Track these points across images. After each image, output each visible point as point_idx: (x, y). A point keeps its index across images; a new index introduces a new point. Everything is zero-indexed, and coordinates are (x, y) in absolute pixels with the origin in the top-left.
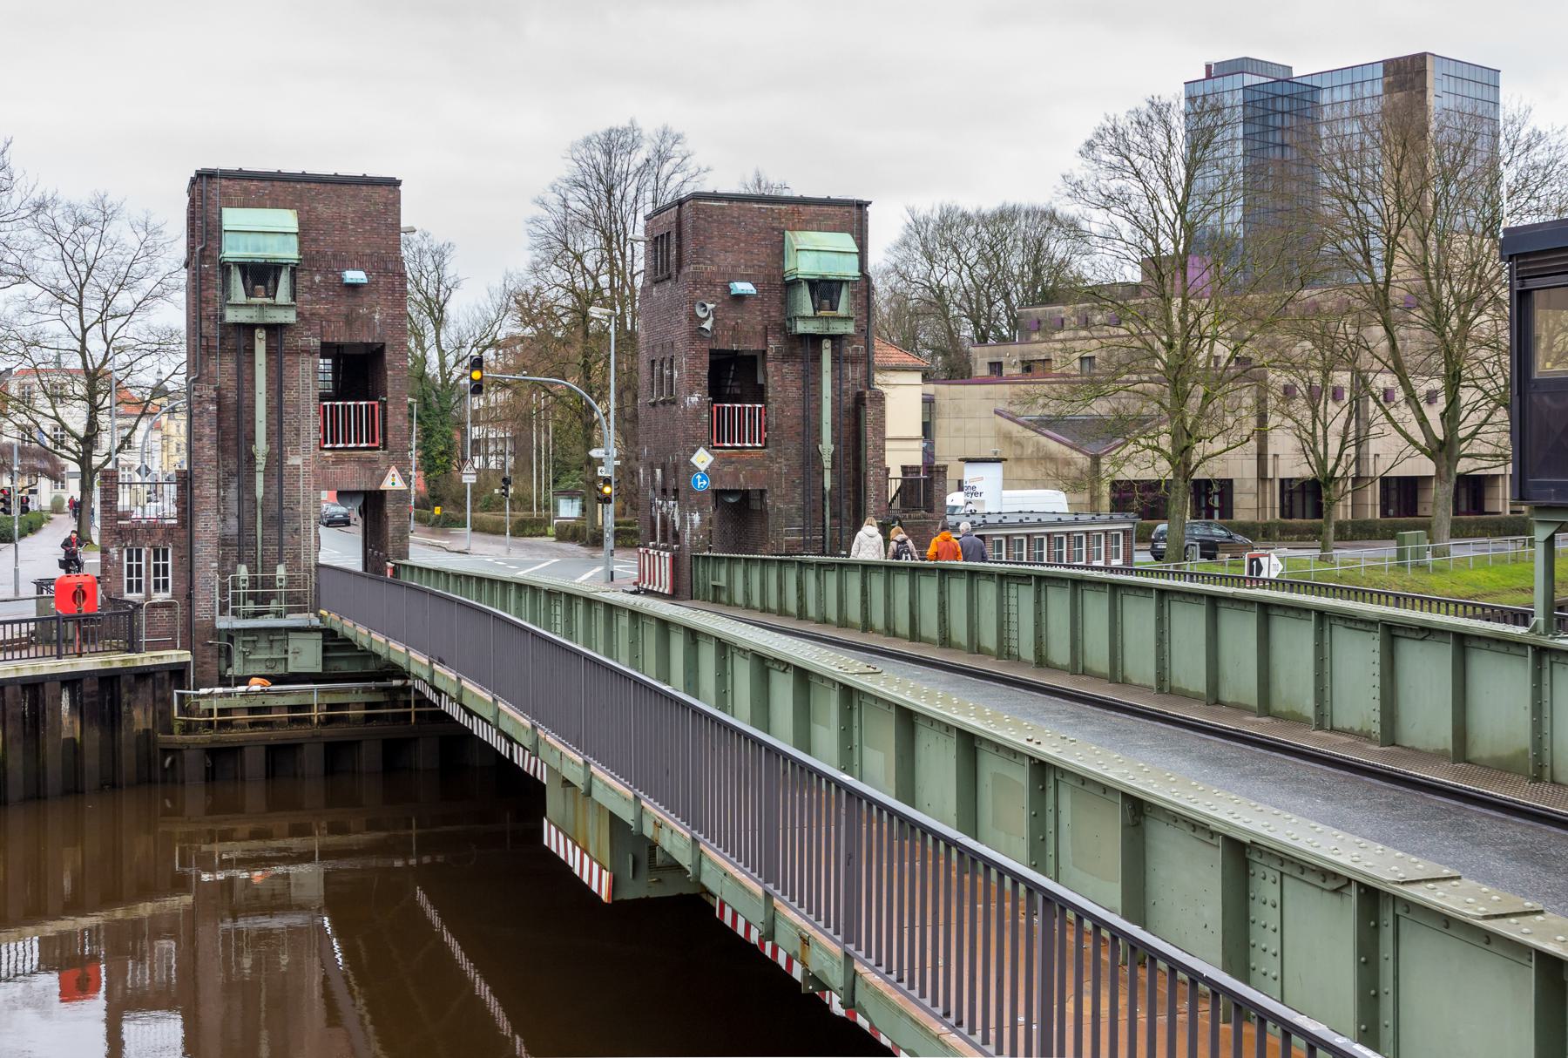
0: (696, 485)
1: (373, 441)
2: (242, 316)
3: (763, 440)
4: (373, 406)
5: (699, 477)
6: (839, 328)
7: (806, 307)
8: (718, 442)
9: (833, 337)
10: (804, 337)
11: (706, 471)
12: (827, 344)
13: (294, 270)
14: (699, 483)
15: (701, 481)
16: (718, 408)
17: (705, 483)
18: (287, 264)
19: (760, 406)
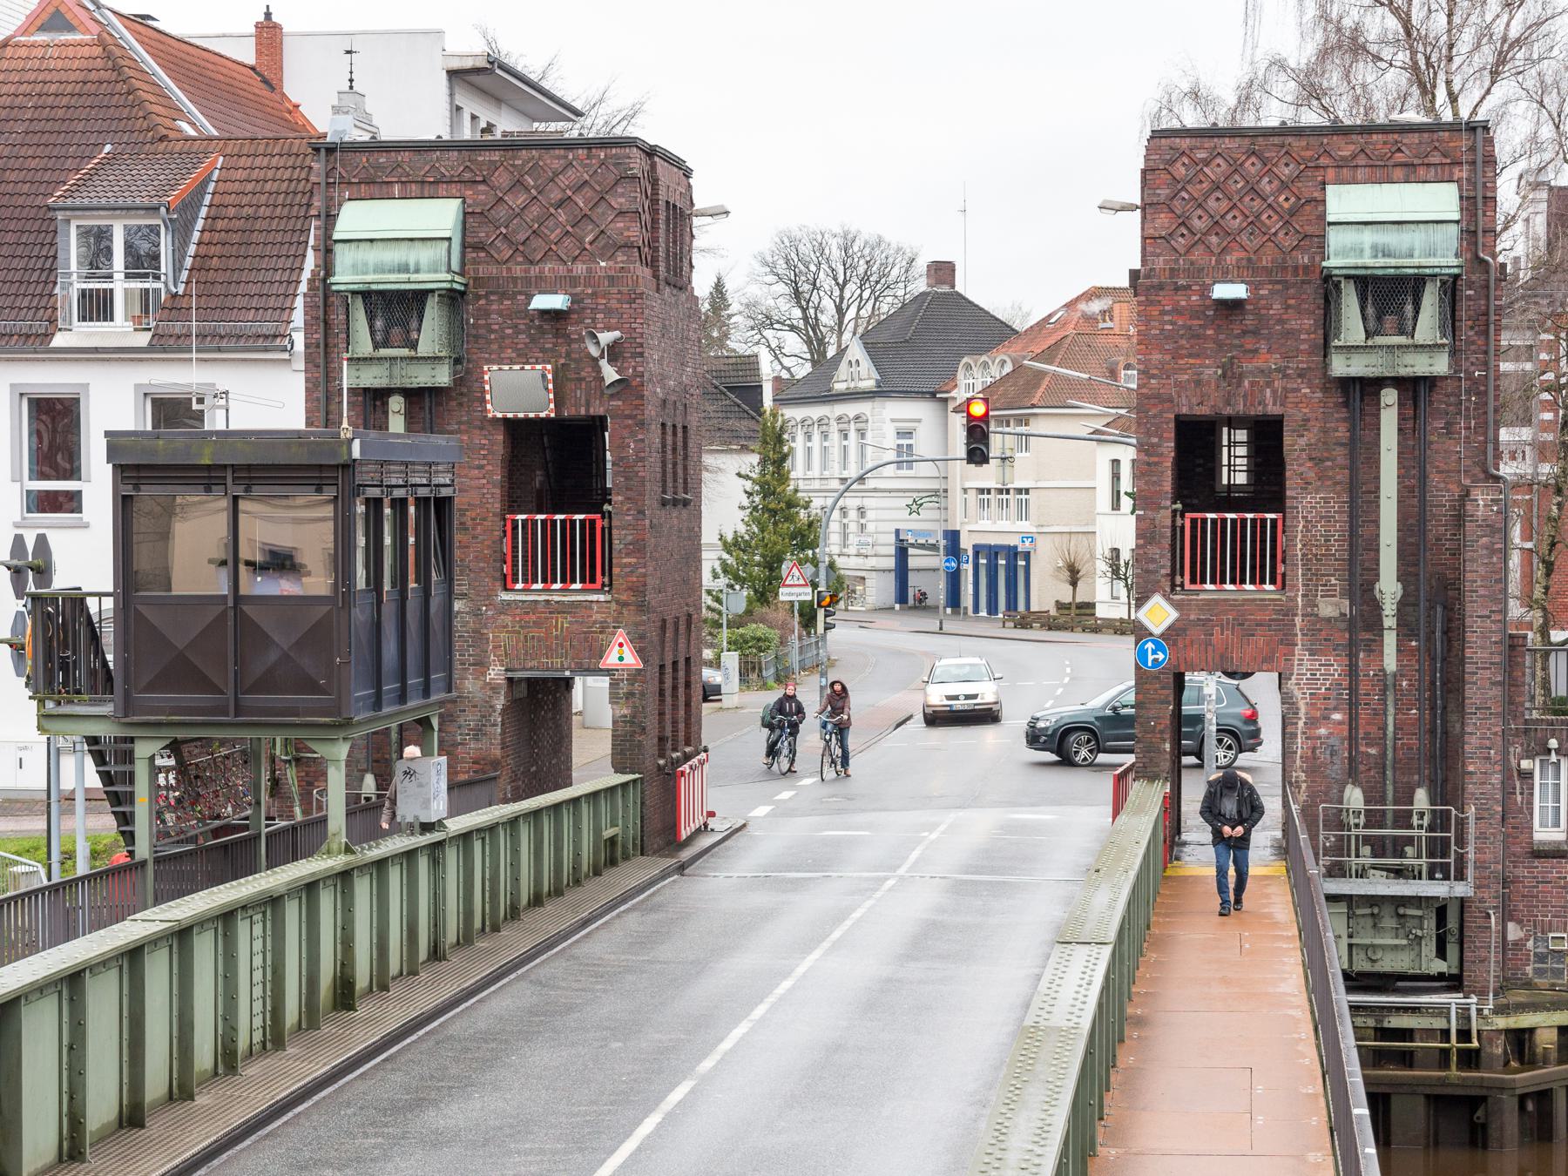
0: (1146, 666)
1: (593, 580)
2: (373, 377)
3: (1279, 578)
4: (593, 522)
5: (1150, 646)
6: (1420, 365)
7: (1352, 326)
8: (1193, 581)
9: (1399, 382)
10: (1346, 383)
11: (1162, 636)
12: (1389, 396)
13: (453, 299)
14: (1151, 658)
15: (1154, 652)
16: (1194, 521)
17: (1161, 656)
18: (432, 291)
19: (1273, 516)
